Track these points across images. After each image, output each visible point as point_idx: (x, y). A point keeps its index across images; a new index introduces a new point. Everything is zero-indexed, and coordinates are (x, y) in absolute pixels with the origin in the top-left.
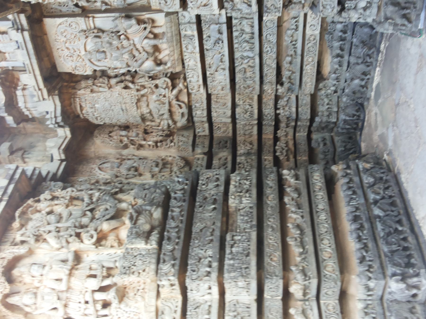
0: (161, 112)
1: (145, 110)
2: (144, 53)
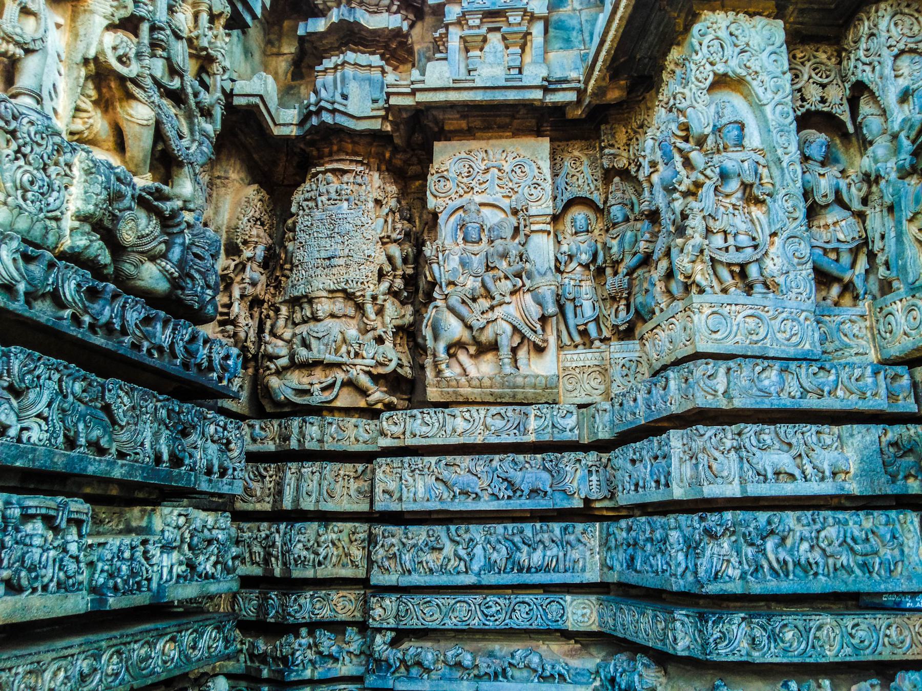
0: (314, 344)
1: (324, 307)
2: (483, 322)
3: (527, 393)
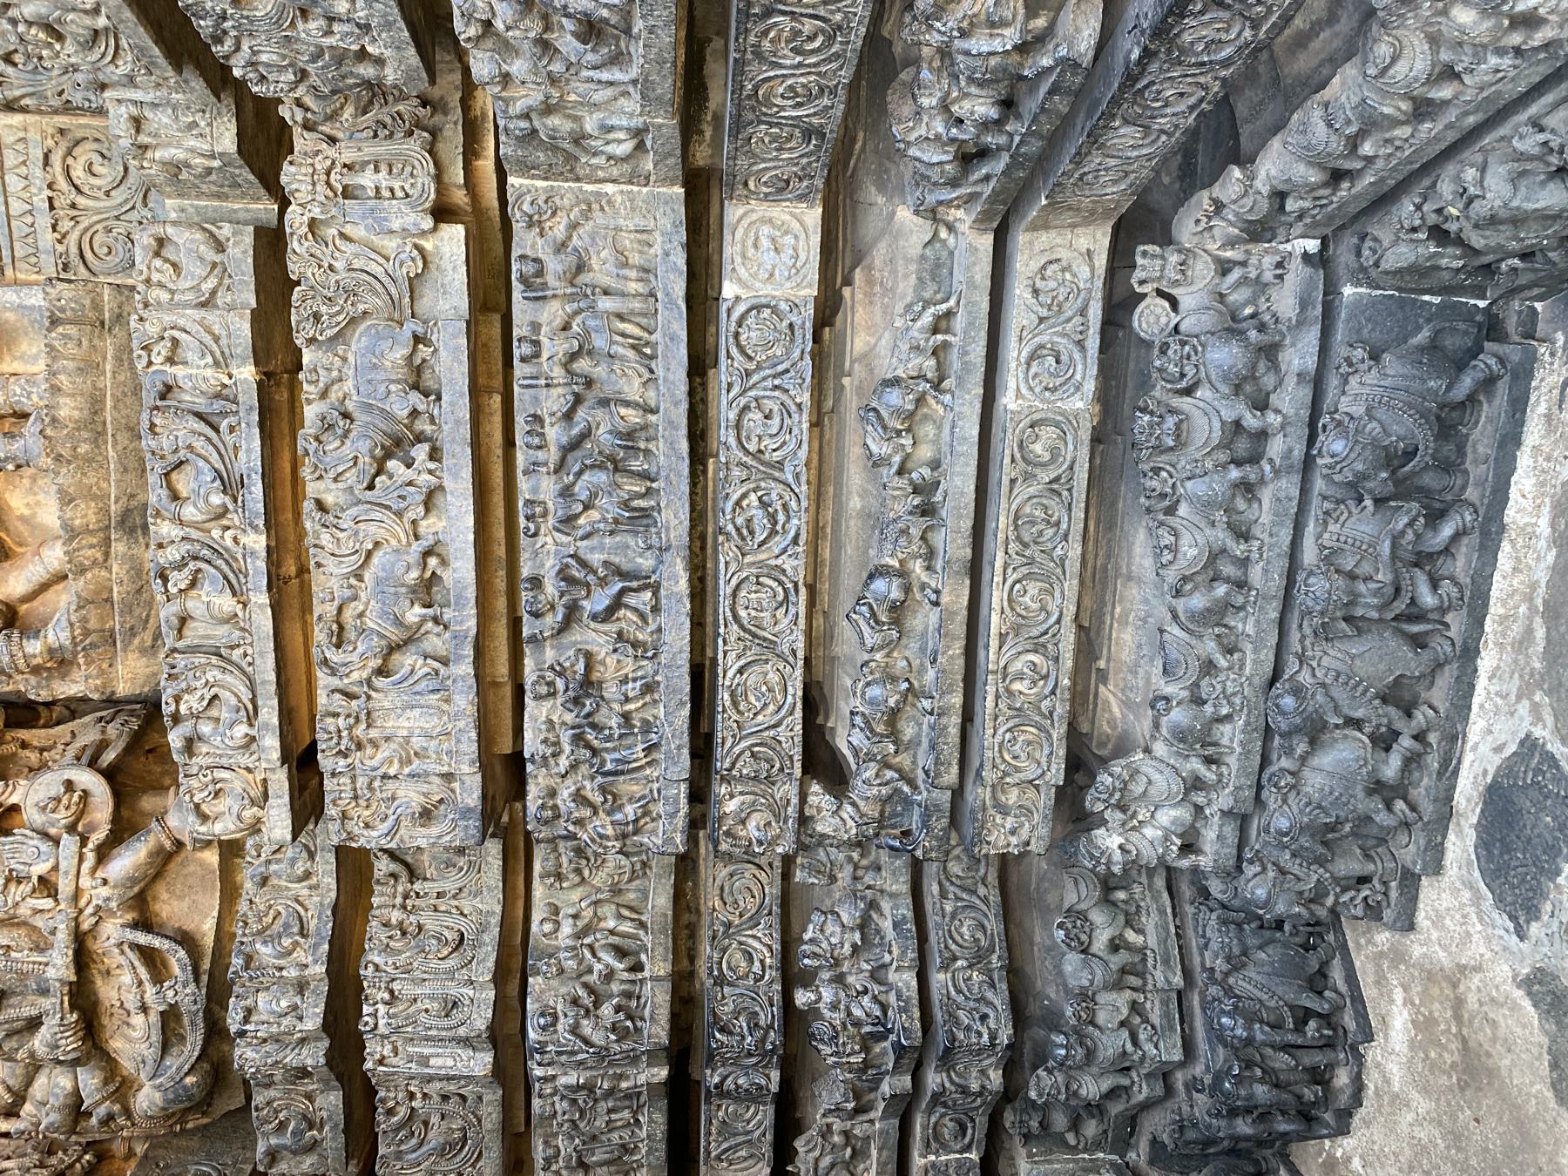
3: (116, 385)
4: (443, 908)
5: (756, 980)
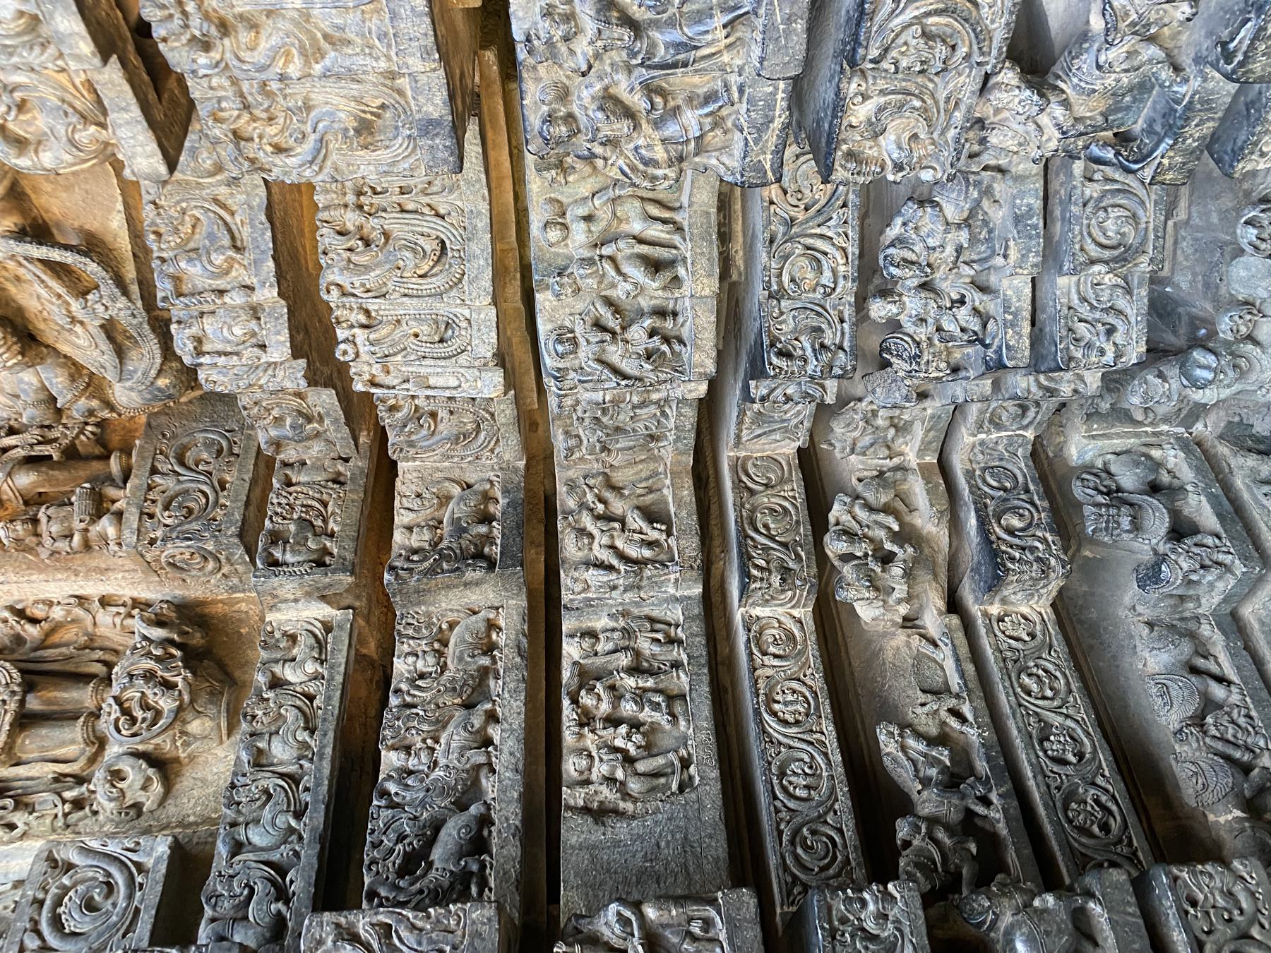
4: (410, 206)
5: (826, 295)
